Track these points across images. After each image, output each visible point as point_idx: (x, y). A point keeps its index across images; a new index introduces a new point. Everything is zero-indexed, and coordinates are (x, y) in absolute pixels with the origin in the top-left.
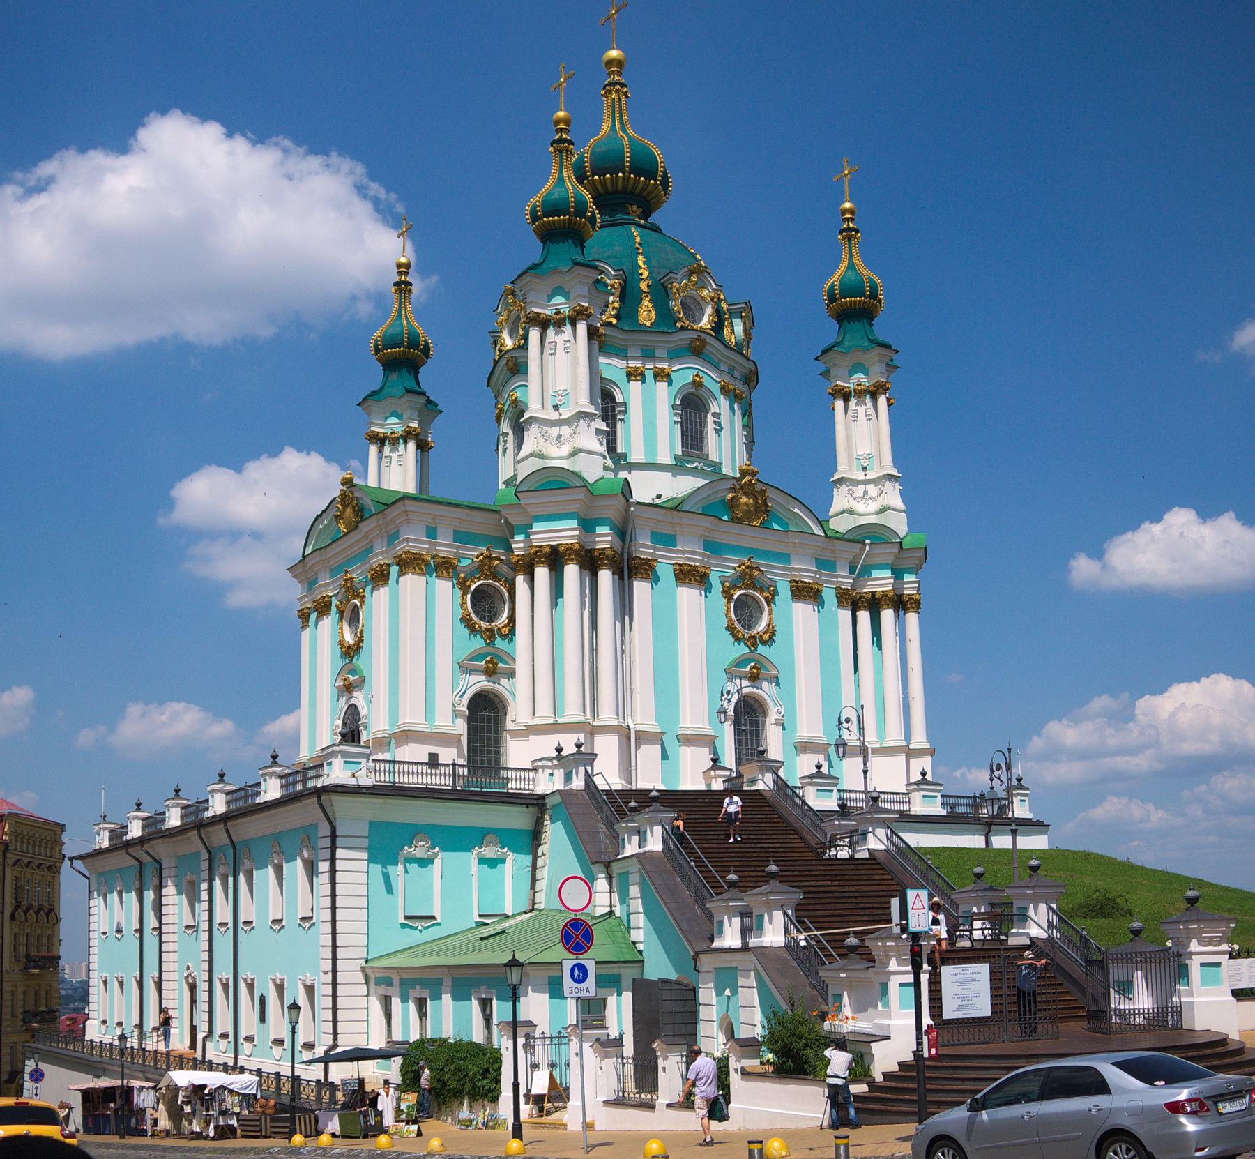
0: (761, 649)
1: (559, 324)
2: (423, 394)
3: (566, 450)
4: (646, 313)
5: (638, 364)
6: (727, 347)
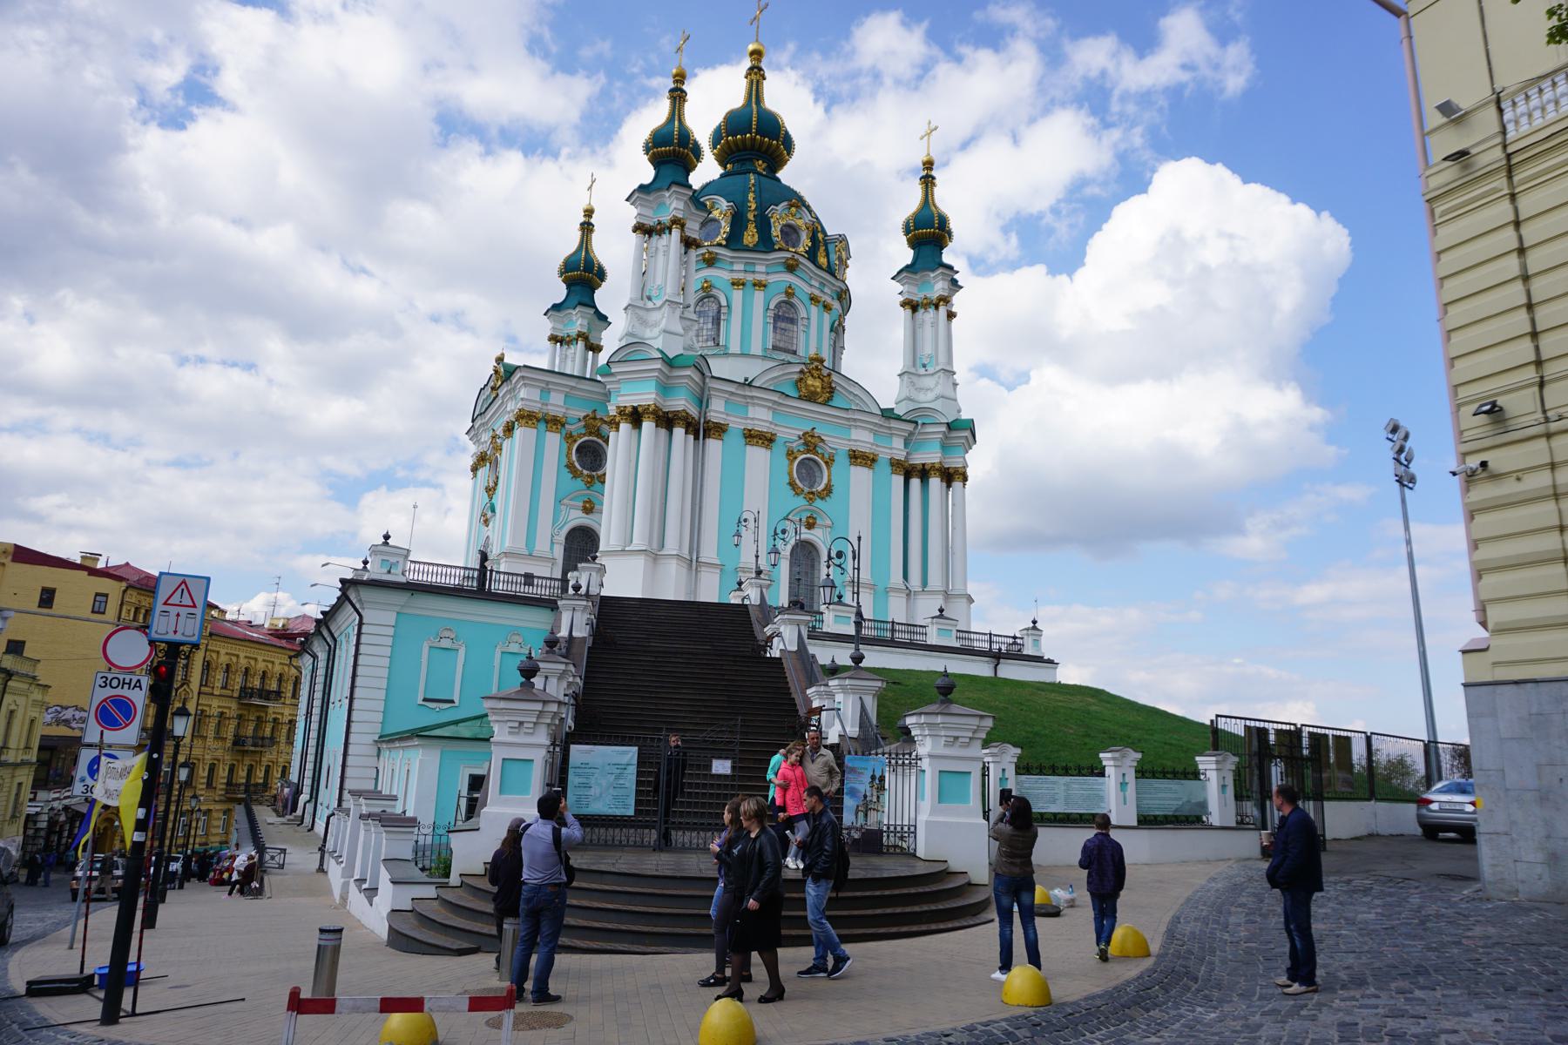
0: (818, 503)
1: (660, 232)
2: (594, 307)
3: (656, 331)
4: (750, 236)
5: (741, 276)
6: (820, 267)
